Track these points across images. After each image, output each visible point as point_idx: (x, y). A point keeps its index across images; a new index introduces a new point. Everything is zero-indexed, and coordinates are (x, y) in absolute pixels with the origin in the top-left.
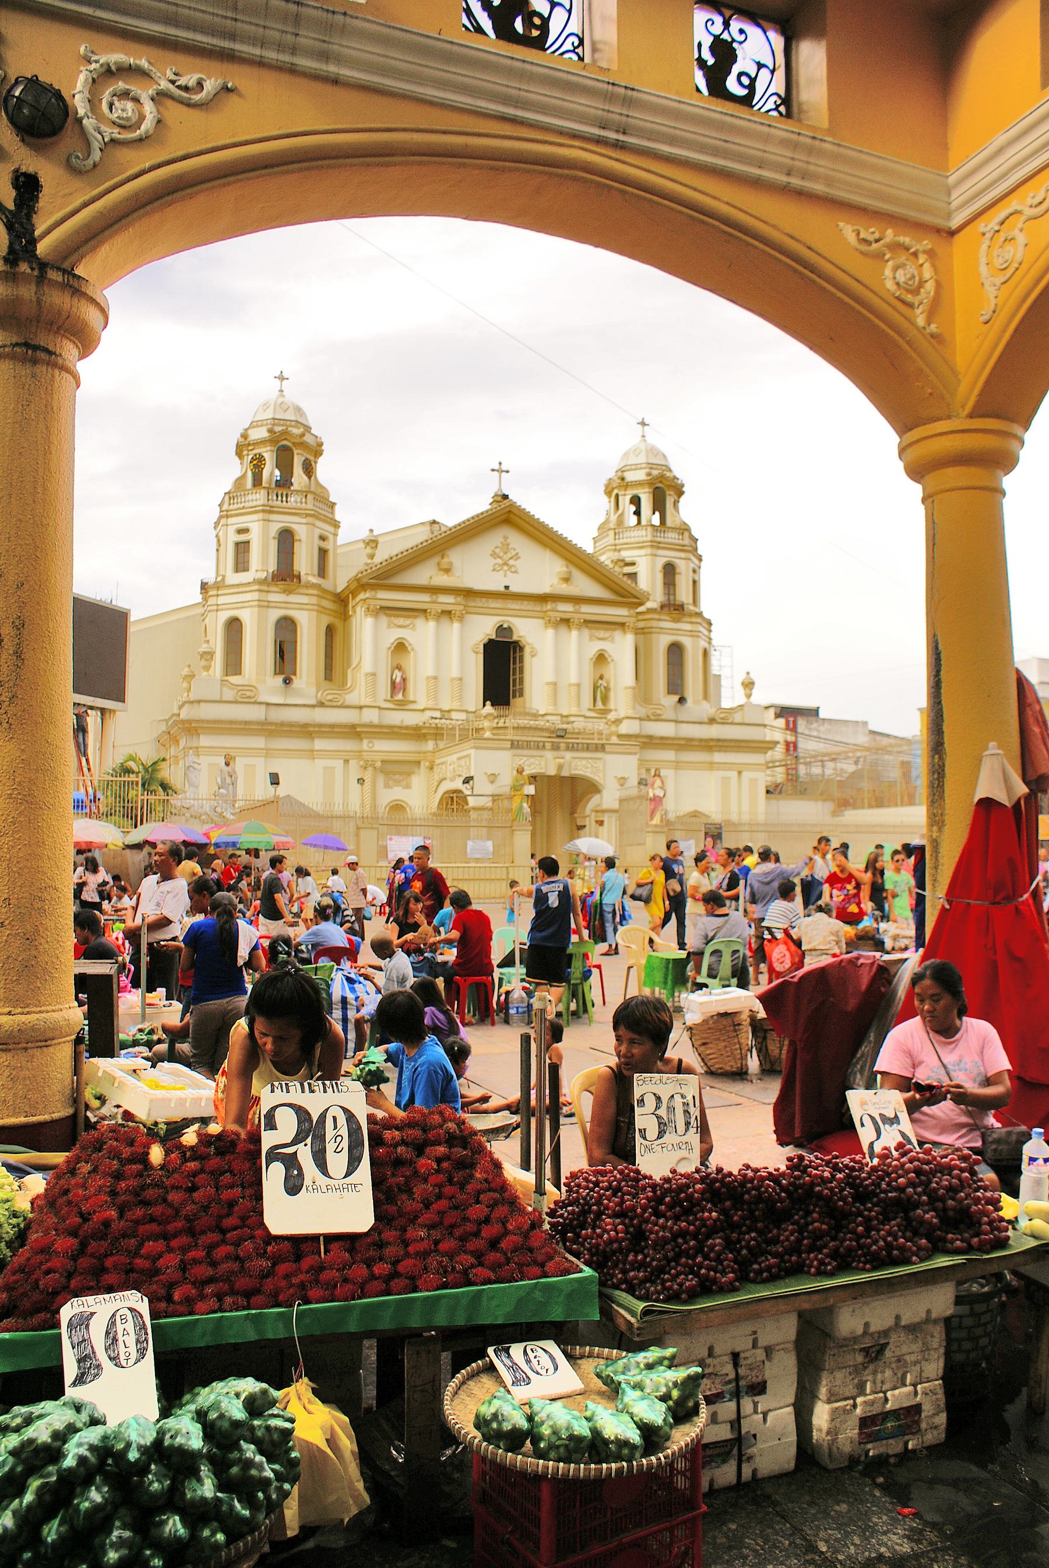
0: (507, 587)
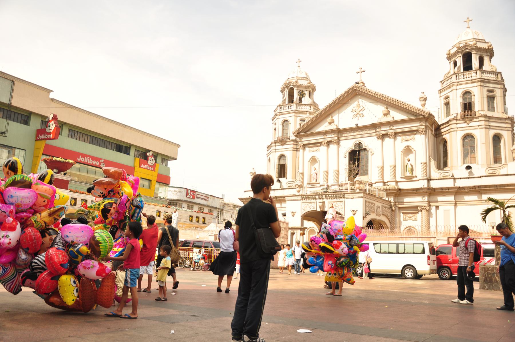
0: (357, 125)
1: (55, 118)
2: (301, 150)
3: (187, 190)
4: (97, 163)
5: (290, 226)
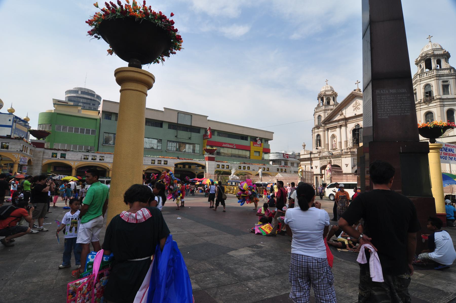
1: (210, 129)
2: (326, 132)
3: (284, 154)
4: (232, 146)
5: (315, 173)
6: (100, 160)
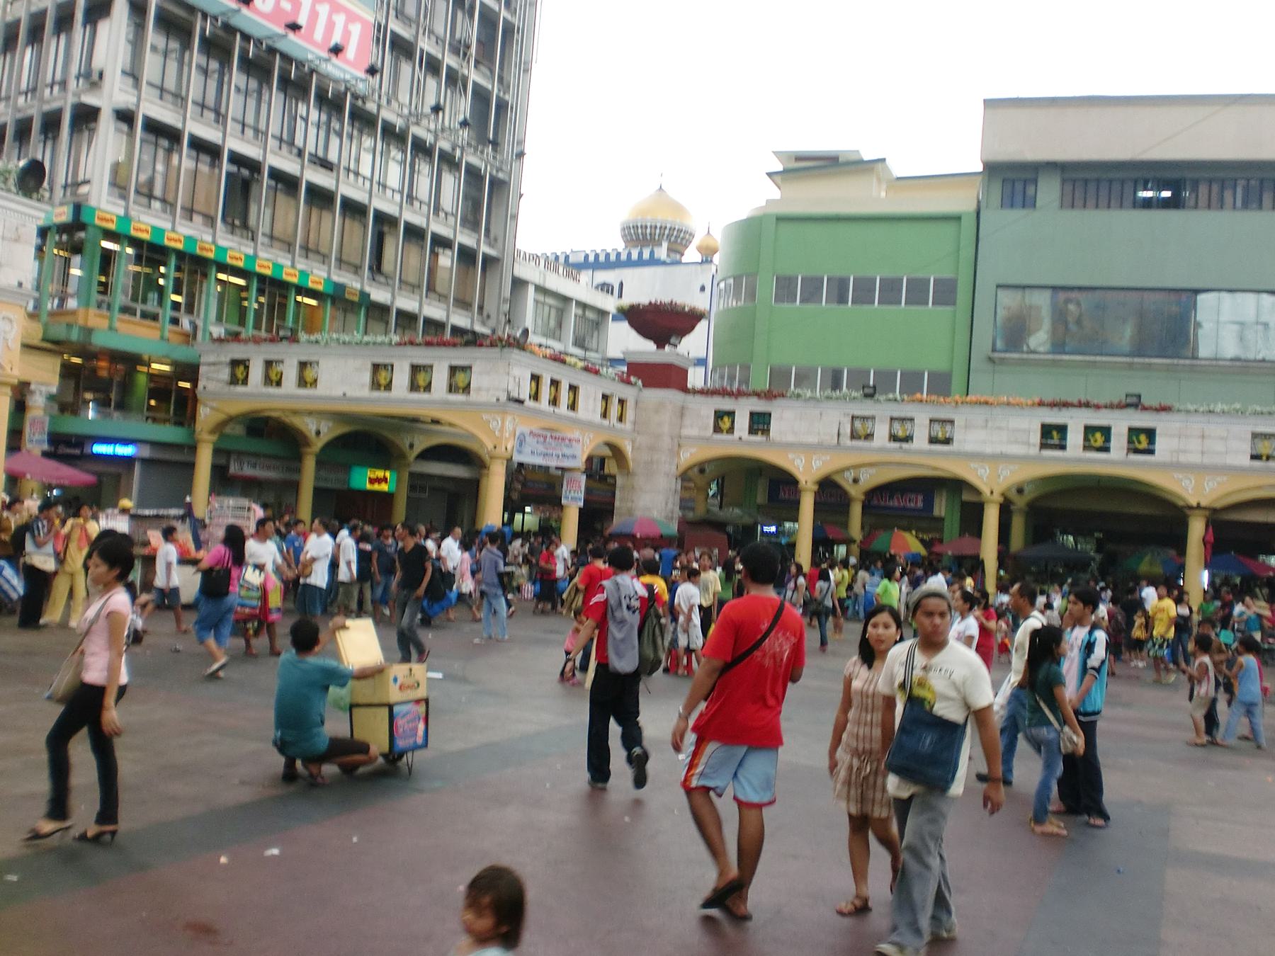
6: (894, 438)
